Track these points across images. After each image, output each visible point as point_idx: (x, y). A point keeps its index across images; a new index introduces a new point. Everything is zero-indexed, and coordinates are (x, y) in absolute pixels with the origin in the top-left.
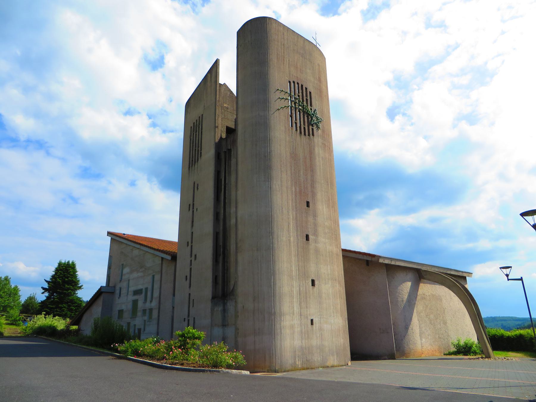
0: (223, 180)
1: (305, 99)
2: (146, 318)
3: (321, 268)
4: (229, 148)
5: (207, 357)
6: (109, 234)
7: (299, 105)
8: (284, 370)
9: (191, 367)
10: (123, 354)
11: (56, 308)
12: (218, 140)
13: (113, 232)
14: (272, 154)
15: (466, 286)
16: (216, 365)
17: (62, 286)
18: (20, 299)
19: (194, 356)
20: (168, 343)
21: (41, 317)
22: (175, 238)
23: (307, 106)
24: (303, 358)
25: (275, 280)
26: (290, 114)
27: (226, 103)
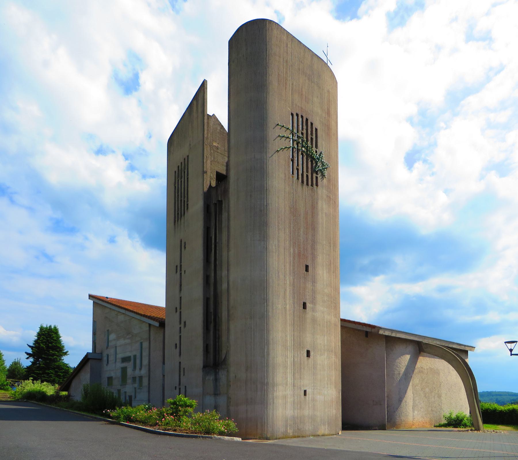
0: (213, 237)
1: (309, 139)
2: (136, 385)
3: (317, 338)
4: (220, 200)
5: (199, 424)
6: (90, 297)
7: (303, 146)
8: (275, 438)
9: (184, 433)
10: (116, 419)
11: (43, 374)
12: (207, 189)
13: (96, 296)
14: (269, 207)
15: (467, 360)
16: (208, 432)
17: (46, 352)
18: (5, 364)
19: (186, 423)
20: (160, 411)
21: (29, 383)
22: (162, 304)
23: (312, 147)
24: (294, 427)
25: (269, 350)
26: (291, 157)
27: (215, 142)
